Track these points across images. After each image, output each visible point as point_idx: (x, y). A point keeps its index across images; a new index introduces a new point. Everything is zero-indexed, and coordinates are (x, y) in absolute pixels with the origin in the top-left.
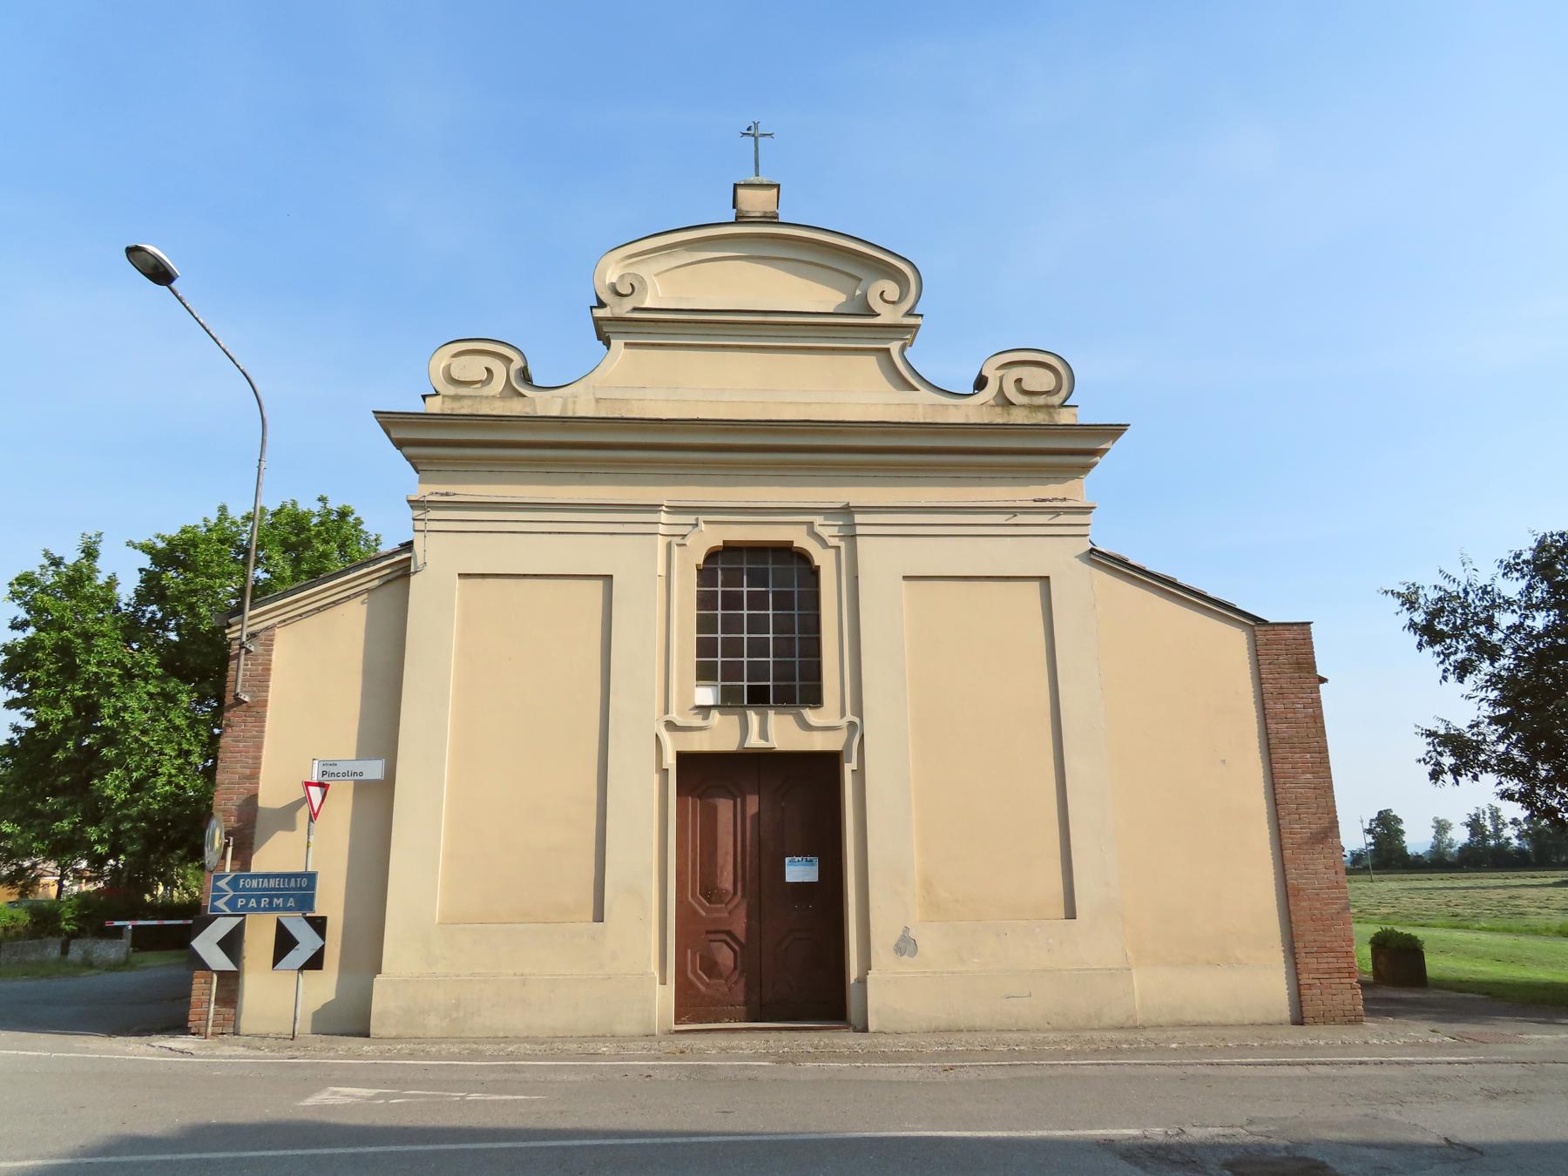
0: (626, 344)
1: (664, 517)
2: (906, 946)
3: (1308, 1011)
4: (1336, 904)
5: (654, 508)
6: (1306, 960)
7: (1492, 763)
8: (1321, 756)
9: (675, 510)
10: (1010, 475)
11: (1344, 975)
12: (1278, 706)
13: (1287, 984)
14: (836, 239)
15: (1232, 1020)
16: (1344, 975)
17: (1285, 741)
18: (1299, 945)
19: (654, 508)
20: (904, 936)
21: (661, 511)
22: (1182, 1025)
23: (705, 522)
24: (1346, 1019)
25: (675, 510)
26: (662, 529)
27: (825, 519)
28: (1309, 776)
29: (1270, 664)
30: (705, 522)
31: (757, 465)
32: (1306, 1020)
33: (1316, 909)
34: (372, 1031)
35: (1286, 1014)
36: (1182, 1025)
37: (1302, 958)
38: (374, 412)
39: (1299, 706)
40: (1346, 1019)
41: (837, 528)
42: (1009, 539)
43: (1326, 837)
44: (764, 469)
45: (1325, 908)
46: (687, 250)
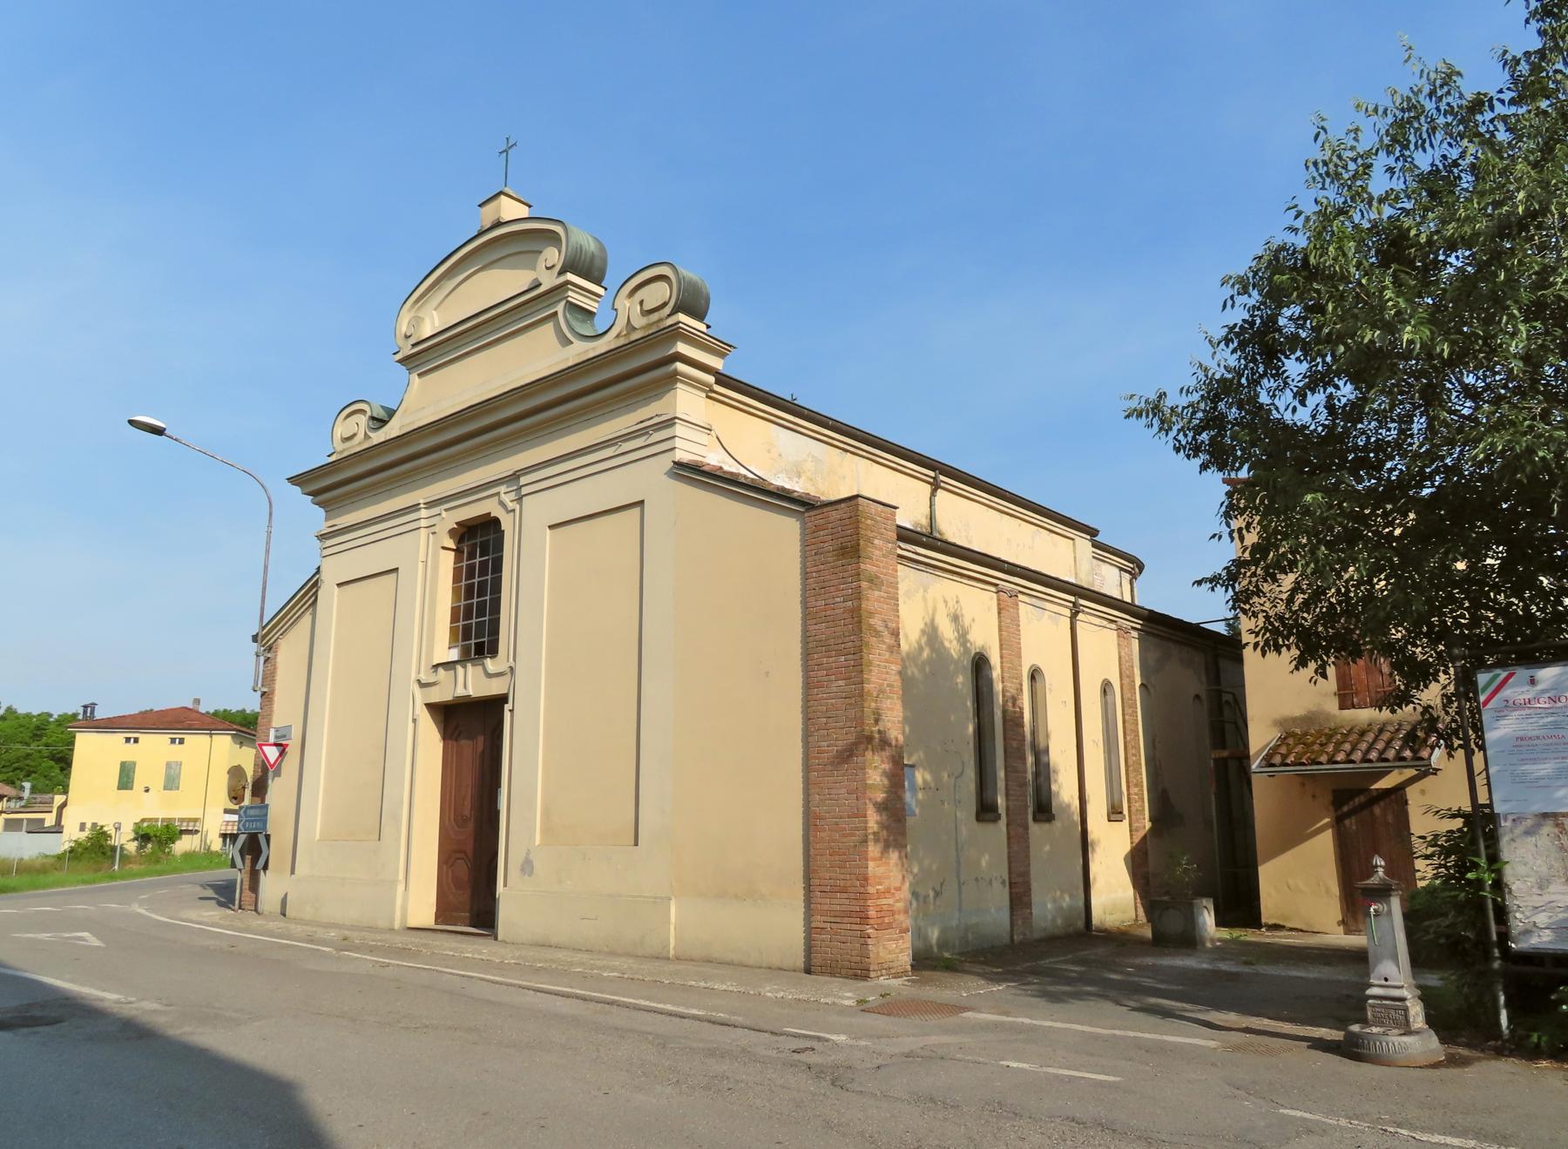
0: (419, 375)
1: (424, 513)
2: (527, 867)
3: (817, 959)
4: (854, 835)
5: (415, 508)
6: (819, 900)
7: (1487, 405)
8: (855, 657)
9: (431, 504)
10: (641, 398)
11: (854, 920)
12: (819, 603)
13: (804, 926)
14: (518, 226)
15: (751, 962)
16: (854, 920)
17: (822, 643)
18: (815, 882)
19: (415, 508)
20: (526, 858)
21: (420, 508)
22: (710, 961)
23: (446, 510)
24: (851, 972)
25: (431, 504)
26: (423, 523)
27: (507, 487)
28: (841, 683)
29: (816, 554)
30: (446, 510)
31: (389, 480)
32: (813, 969)
33: (834, 841)
34: (287, 914)
35: (800, 962)
36: (710, 961)
37: (1126, 709)
38: (288, 479)
39: (838, 599)
40: (851, 972)
41: (514, 493)
42: (618, 470)
43: (851, 756)
44: (557, 424)
45: (844, 840)
46: (449, 279)
